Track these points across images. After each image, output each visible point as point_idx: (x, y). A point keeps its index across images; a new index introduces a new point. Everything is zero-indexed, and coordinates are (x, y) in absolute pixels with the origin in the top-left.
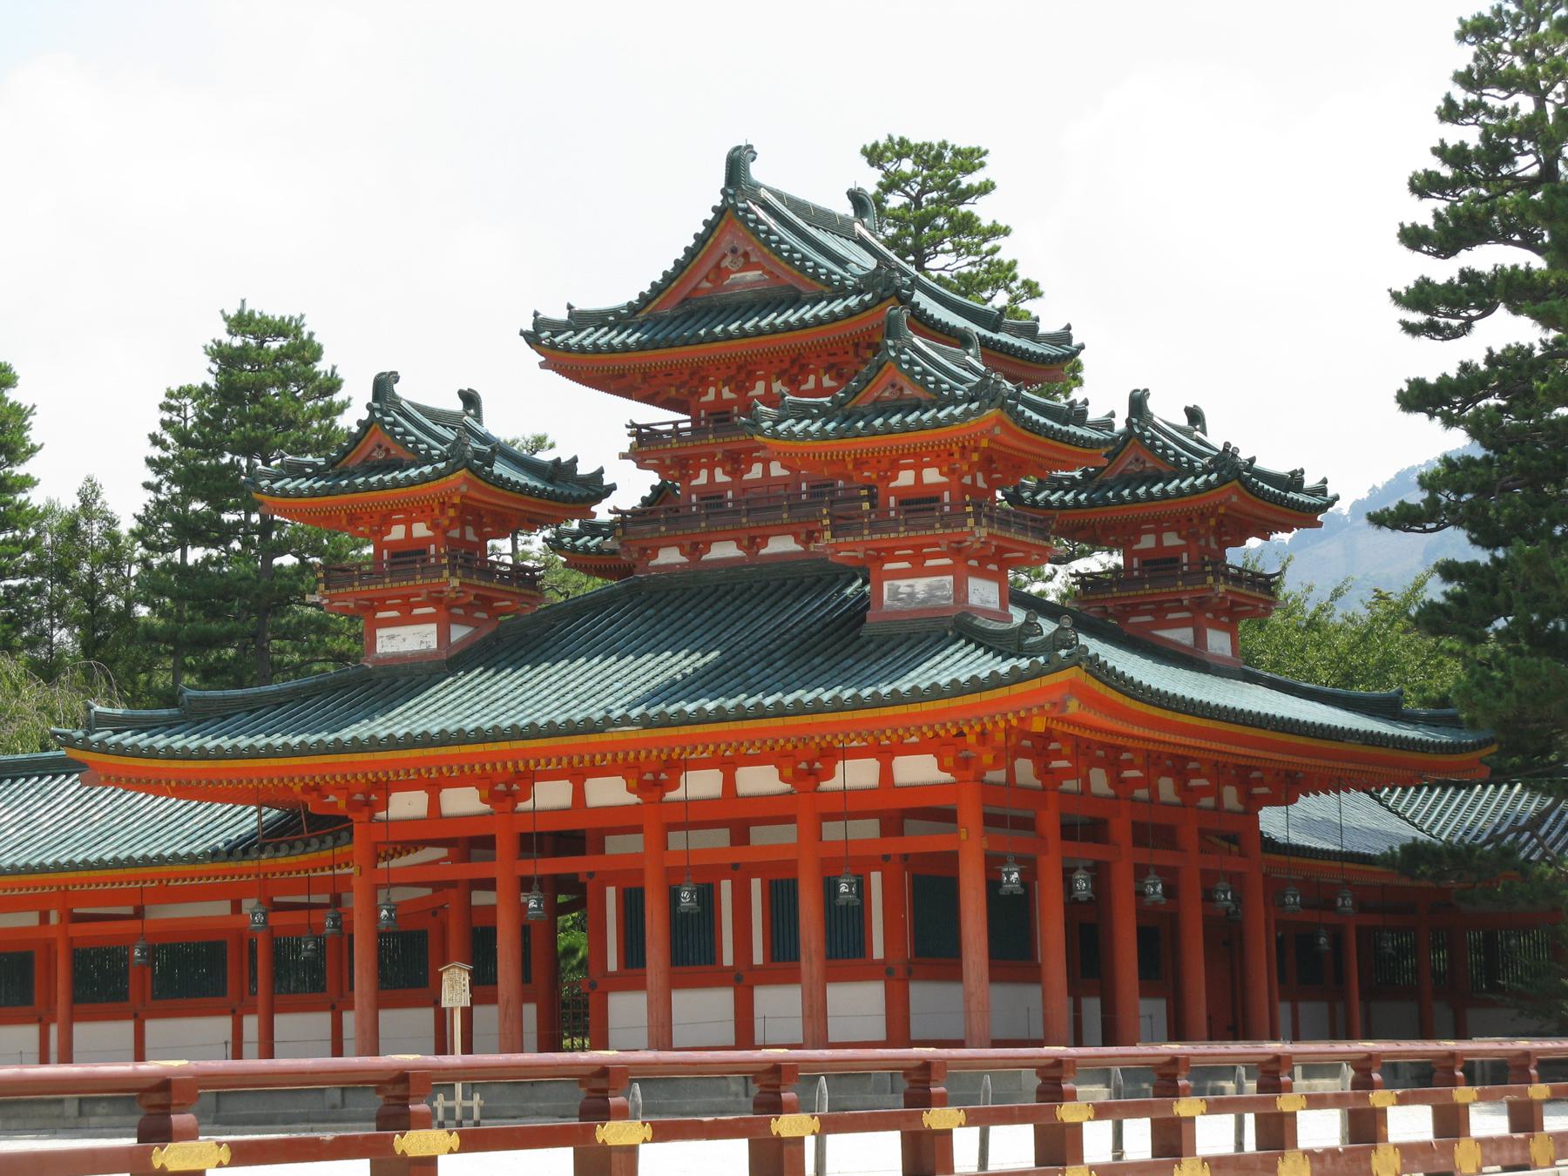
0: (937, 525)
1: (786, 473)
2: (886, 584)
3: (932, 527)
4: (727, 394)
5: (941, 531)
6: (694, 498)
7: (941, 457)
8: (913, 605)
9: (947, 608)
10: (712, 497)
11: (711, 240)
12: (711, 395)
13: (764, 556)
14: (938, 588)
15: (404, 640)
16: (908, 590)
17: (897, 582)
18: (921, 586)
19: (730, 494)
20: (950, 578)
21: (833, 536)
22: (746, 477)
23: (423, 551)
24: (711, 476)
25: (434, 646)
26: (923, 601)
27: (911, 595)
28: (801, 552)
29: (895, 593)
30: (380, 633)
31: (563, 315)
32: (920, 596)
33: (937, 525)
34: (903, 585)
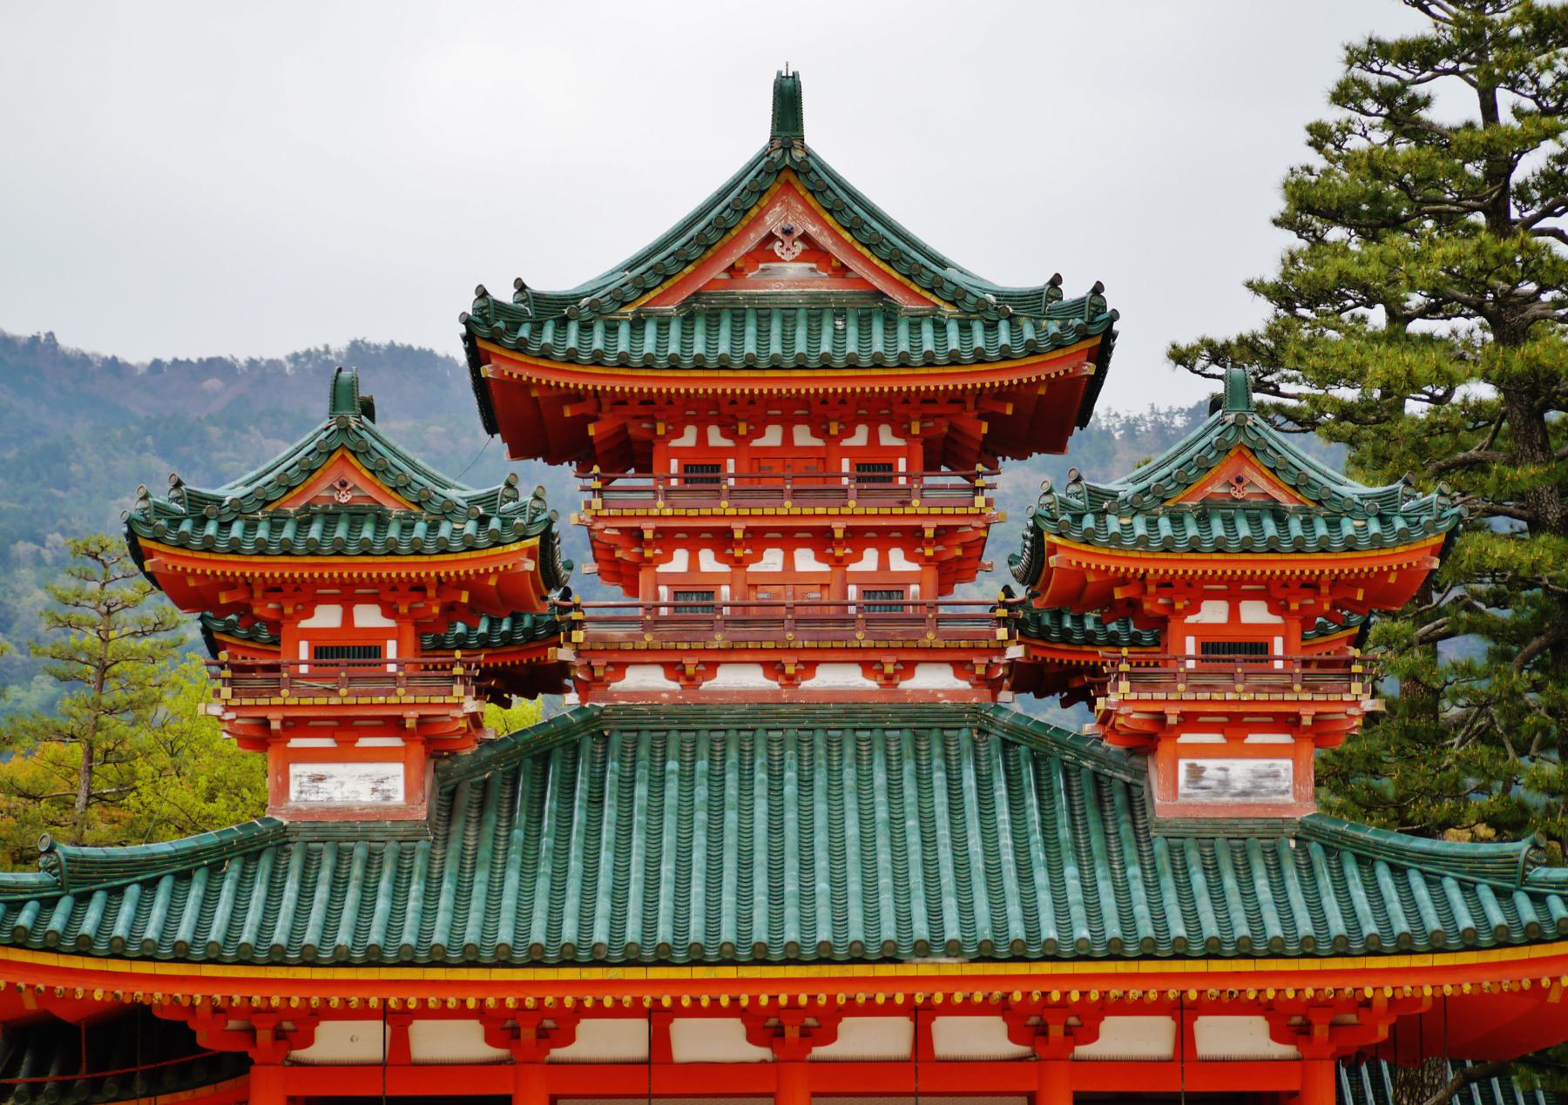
0: (1297, 687)
1: (825, 568)
2: (1183, 765)
3: (1288, 688)
4: (715, 438)
5: (1308, 697)
6: (664, 591)
7: (1274, 592)
8: (1226, 799)
9: (1287, 807)
10: (693, 594)
11: (754, 211)
12: (689, 438)
13: (810, 692)
14: (1267, 776)
15: (342, 784)
16: (1221, 774)
17: (1200, 763)
18: (1241, 770)
19: (725, 591)
20: (1288, 763)
21: (1131, 690)
22: (752, 568)
23: (376, 652)
24: (694, 561)
25: (399, 798)
26: (1244, 793)
27: (1225, 783)
28: (870, 692)
29: (1196, 774)
30: (295, 769)
31: (504, 294)
32: (1240, 785)
33: (1297, 687)
34: (1211, 766)
